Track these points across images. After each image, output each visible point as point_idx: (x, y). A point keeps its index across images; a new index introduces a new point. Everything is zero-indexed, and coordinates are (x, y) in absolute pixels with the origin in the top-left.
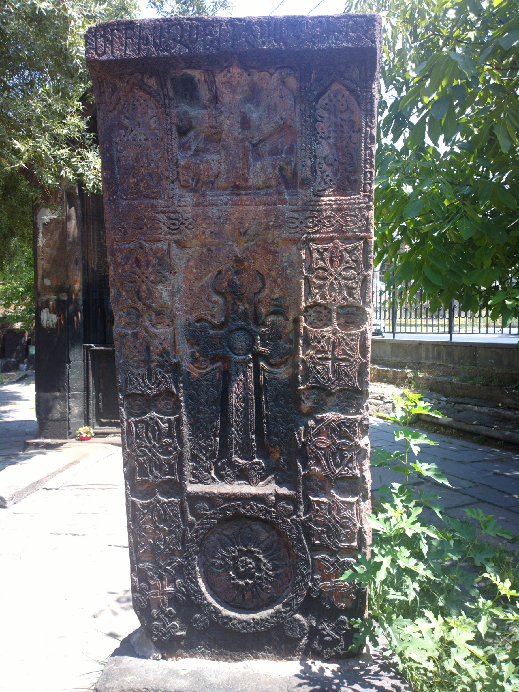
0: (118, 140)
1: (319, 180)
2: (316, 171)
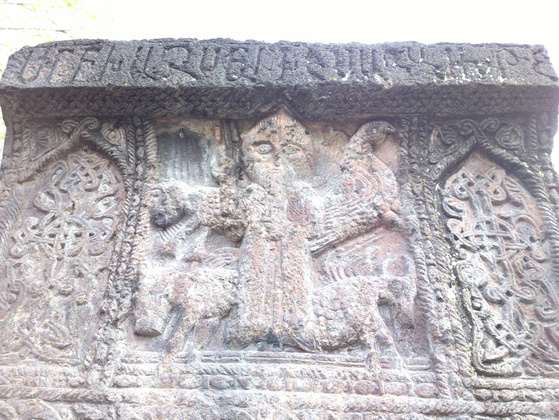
0: (18, 234)
1: (480, 335)
2: (468, 315)
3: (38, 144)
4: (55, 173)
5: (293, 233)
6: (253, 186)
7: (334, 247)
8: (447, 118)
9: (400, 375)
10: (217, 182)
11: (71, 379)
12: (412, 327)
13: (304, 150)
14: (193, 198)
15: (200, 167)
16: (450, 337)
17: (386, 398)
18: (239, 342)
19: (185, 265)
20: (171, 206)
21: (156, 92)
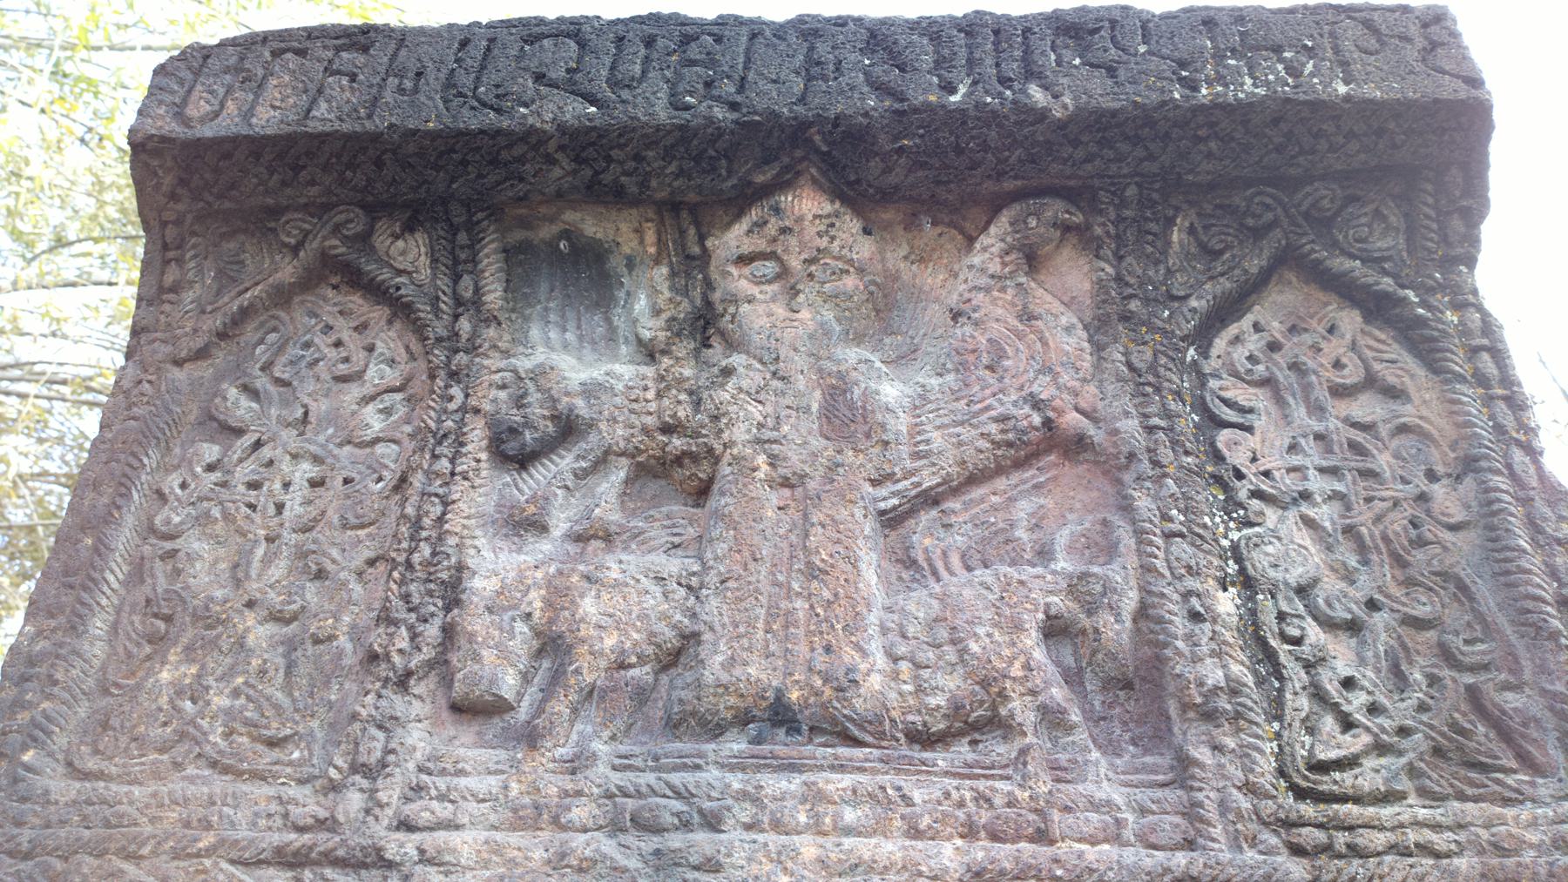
0: (172, 482)
2: (1270, 656)
3: (220, 273)
4: (261, 341)
5: (834, 467)
6: (737, 360)
7: (936, 502)
8: (1212, 187)
9: (1100, 795)
10: (649, 352)
11: (295, 811)
12: (1128, 685)
13: (861, 271)
14: (590, 391)
15: (608, 320)
16: (1223, 703)
17: (1063, 849)
18: (703, 723)
19: (572, 548)
20: (537, 411)
21: (502, 141)
